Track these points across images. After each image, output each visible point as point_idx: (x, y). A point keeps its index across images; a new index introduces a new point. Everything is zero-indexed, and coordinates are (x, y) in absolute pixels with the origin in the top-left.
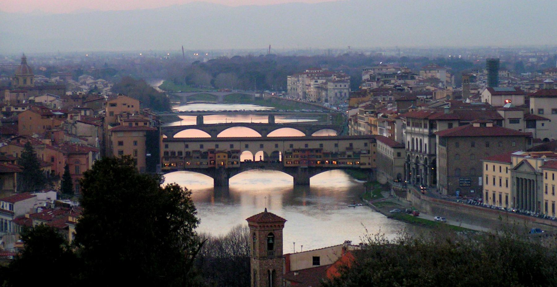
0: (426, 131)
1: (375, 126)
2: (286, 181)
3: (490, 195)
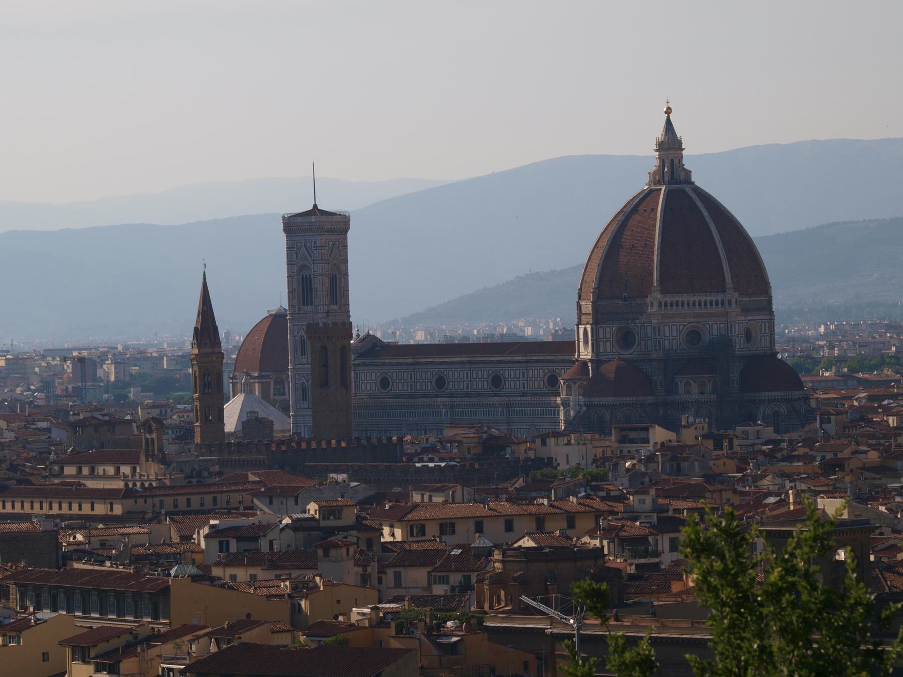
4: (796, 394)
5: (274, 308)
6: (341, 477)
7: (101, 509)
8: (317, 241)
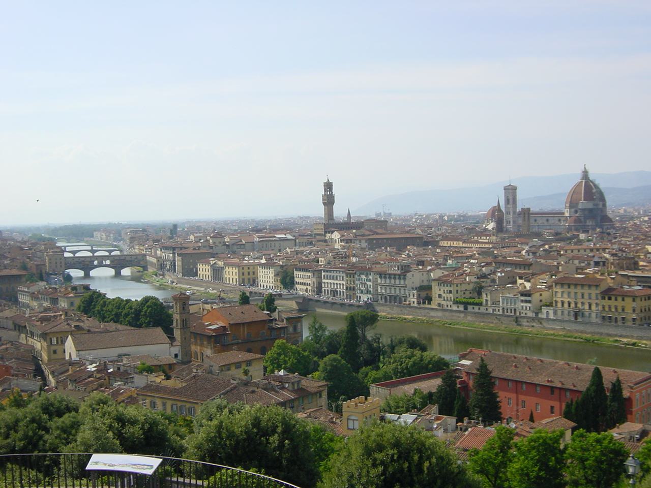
0: (171, 252)
1: (143, 251)
2: (112, 272)
3: (201, 275)
4: (611, 223)
5: (494, 206)
6: (537, 240)
7: (487, 246)
8: (511, 192)
